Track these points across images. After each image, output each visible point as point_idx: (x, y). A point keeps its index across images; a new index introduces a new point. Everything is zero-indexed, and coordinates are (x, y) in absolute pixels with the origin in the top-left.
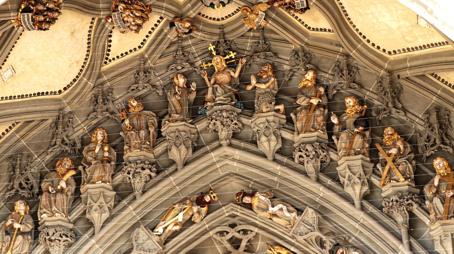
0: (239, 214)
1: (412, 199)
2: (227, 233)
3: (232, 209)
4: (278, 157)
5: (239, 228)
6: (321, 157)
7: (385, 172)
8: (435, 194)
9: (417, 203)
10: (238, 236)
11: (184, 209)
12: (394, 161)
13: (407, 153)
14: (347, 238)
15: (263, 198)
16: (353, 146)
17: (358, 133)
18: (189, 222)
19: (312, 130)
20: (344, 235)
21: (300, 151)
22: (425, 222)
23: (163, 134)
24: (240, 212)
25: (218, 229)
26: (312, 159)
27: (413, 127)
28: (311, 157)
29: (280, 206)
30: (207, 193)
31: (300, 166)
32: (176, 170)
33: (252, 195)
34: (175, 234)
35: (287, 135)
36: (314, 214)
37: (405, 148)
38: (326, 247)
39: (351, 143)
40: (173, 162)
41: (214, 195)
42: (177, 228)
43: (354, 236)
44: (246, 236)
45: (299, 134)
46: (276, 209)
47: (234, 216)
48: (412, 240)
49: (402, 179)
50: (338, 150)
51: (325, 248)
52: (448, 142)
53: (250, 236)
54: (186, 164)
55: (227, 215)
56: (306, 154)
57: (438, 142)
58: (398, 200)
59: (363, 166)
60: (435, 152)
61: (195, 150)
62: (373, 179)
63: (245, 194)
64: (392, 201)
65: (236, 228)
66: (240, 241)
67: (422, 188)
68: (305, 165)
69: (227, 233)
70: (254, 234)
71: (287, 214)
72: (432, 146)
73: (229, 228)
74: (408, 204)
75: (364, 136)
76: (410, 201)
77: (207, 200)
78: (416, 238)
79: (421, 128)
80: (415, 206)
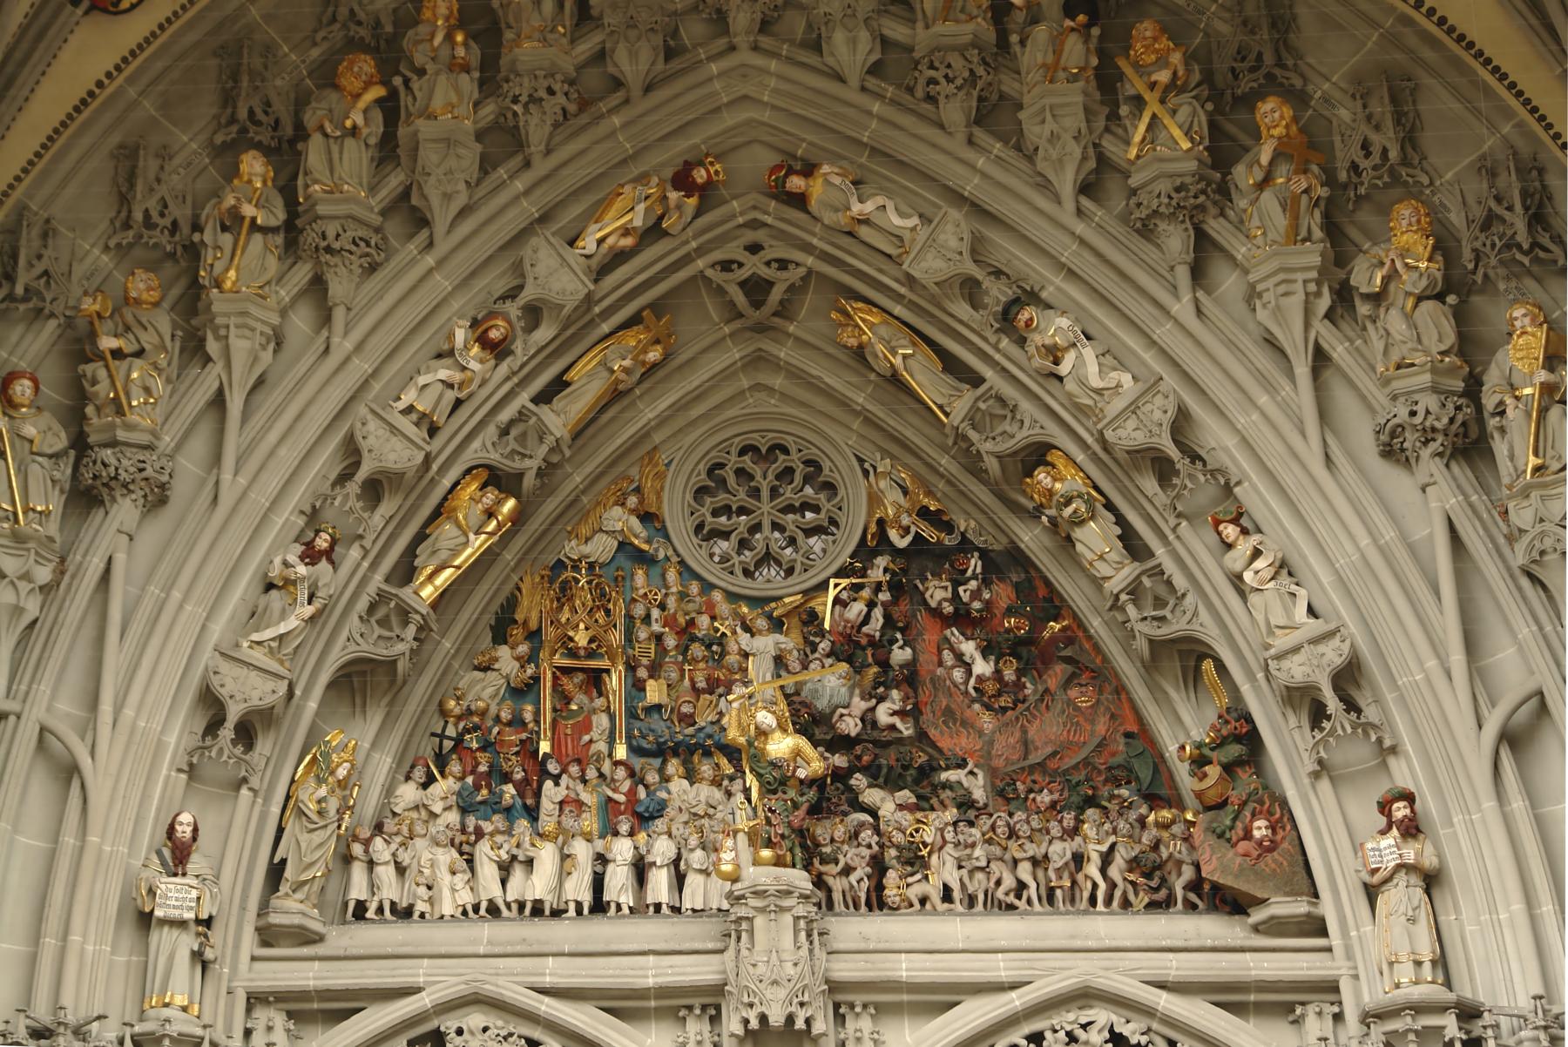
0: (769, 220)
1: (1203, 192)
2: (741, 265)
3: (754, 208)
4: (872, 82)
5: (768, 254)
6: (980, 85)
7: (1142, 128)
8: (1263, 185)
9: (1215, 203)
10: (765, 272)
11: (646, 198)
12: (1162, 101)
13: (1192, 85)
14: (1036, 289)
15: (837, 180)
16: (1062, 62)
17: (1073, 29)
18: (654, 231)
19: (963, 17)
20: (1031, 282)
21: (932, 67)
22: (1235, 253)
23: (594, 12)
24: (773, 212)
25: (718, 255)
26: (959, 88)
27: (1202, 26)
28: (959, 82)
29: (880, 200)
30: (701, 163)
31: (927, 108)
32: (627, 101)
33: (809, 170)
34: (619, 257)
35: (897, 31)
36: (963, 224)
37: (1188, 71)
38: (987, 304)
39: (1058, 53)
40: (617, 83)
41: (718, 167)
42: (628, 242)
43: (1052, 283)
44: (784, 275)
45: (927, 27)
46: (869, 207)
47: (755, 225)
48: (1200, 294)
49: (1186, 145)
50: (1023, 71)
51: (985, 307)
52: (1290, 62)
53: (794, 274)
54: (648, 89)
55: (741, 220)
56: (946, 77)
57: (1269, 59)
58: (1174, 195)
59: (1087, 110)
60: (1260, 86)
61: (670, 54)
62: (1104, 143)
63: (791, 171)
64: (1159, 195)
65: (762, 253)
66: (771, 284)
67: (1226, 173)
68: (941, 106)
69: (741, 265)
70: (802, 271)
71: (896, 221)
72: (1253, 70)
73: (747, 253)
74: (1196, 207)
75: (1087, 39)
76: (1202, 198)
77: (699, 181)
78: (1209, 293)
79: (1223, 28)
80: (1213, 211)
